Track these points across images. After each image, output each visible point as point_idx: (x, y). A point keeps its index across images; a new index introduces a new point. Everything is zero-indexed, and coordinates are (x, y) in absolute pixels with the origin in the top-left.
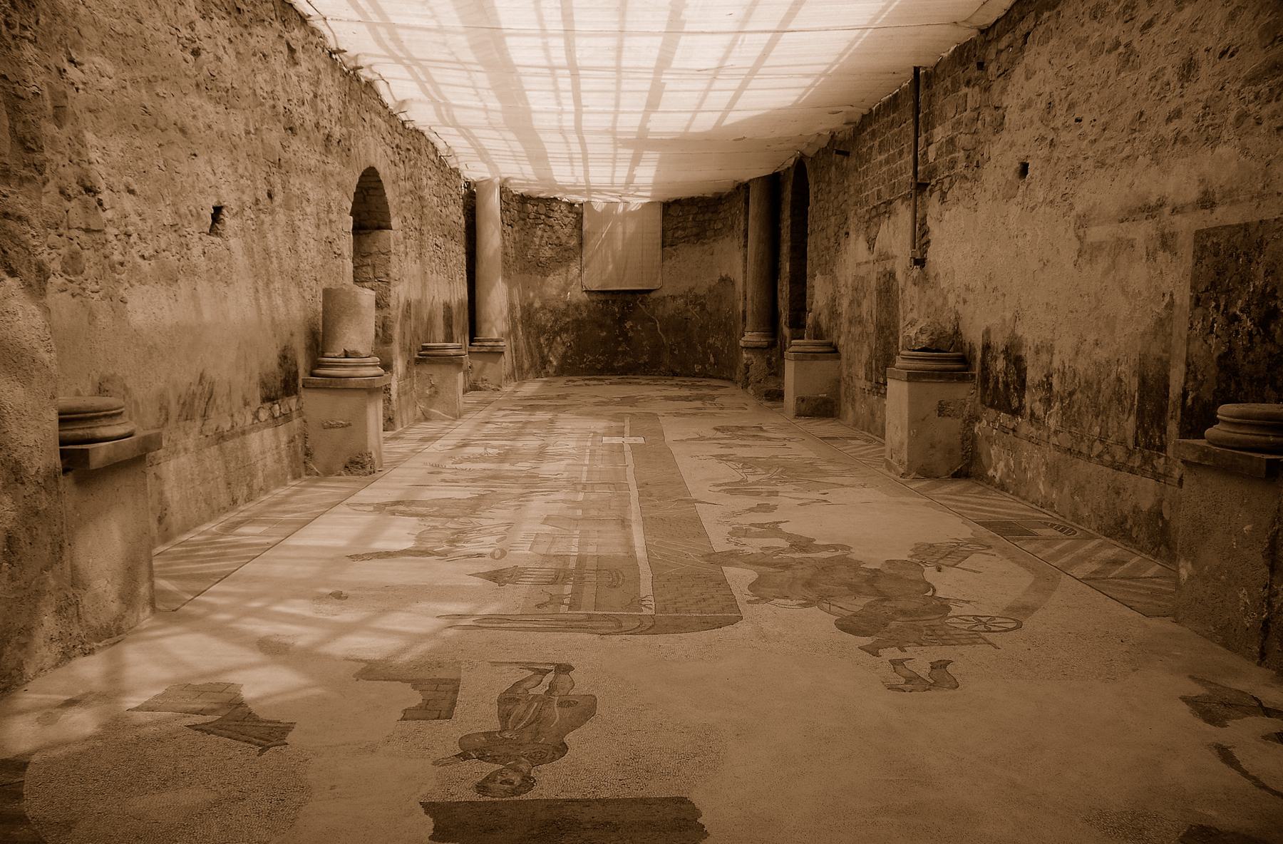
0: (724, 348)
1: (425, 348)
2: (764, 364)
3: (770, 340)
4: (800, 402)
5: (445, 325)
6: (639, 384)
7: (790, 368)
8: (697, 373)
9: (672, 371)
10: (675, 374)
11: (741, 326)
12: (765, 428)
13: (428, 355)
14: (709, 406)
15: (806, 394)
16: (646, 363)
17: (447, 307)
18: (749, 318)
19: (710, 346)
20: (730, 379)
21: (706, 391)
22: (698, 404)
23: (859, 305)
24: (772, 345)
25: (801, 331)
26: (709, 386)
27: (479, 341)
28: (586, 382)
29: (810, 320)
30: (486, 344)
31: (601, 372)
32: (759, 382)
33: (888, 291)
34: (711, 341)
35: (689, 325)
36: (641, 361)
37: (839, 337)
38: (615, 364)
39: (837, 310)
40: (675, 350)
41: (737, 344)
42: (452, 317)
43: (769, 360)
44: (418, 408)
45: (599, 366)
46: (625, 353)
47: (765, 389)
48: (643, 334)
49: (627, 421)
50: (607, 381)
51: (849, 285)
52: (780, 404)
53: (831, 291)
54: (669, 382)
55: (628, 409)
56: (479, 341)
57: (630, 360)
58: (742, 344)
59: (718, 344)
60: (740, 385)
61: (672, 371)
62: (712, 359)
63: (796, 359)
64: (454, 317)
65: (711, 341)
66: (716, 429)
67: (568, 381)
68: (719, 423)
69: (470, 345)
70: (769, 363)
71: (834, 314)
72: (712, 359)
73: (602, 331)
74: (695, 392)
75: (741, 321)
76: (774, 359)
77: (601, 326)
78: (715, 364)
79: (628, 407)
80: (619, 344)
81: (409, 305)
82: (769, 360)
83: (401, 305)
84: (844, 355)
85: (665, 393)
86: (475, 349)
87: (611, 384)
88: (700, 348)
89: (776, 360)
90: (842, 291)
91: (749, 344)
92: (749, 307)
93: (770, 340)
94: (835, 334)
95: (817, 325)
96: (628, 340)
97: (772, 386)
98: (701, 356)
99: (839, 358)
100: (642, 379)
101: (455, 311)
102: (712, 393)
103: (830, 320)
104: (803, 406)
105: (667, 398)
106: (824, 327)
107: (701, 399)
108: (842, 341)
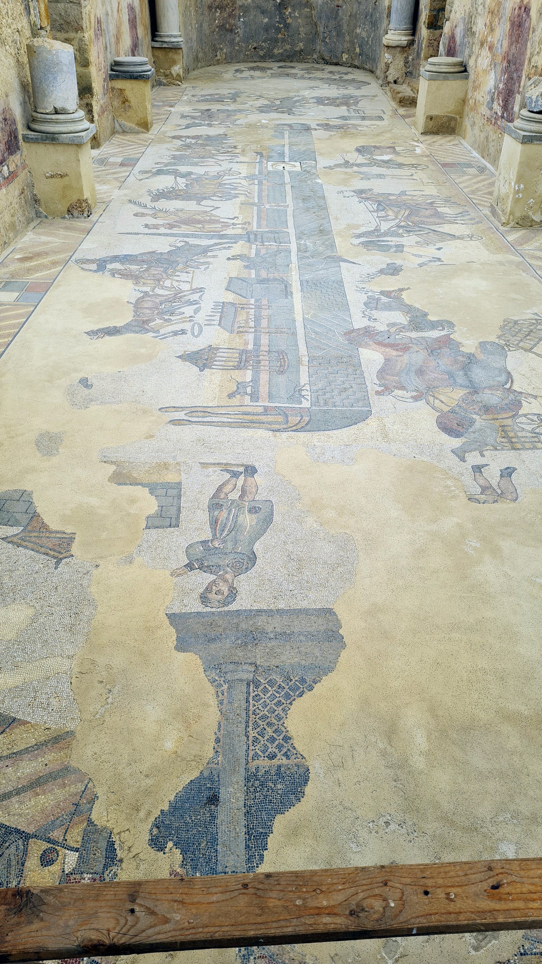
0: (368, 38)
1: (117, 64)
2: (402, 63)
3: (411, 38)
4: (429, 120)
5: (130, 28)
6: (294, 76)
7: (423, 85)
8: (344, 63)
9: (323, 59)
10: (327, 63)
11: (385, 22)
12: (397, 149)
13: (120, 71)
14: (353, 114)
15: (434, 113)
16: (302, 51)
17: (131, 8)
18: (393, 16)
19: (357, 36)
20: (372, 72)
21: (351, 91)
22: (343, 110)
23: (492, 30)
24: (411, 43)
25: (438, 32)
26: (353, 80)
27: (160, 36)
28: (252, 73)
29: (447, 28)
30: (167, 40)
31: (263, 59)
32: (395, 82)
33: (520, 26)
34: (358, 31)
35: (340, 13)
36: (298, 49)
37: (470, 56)
38: (276, 51)
39: (471, 28)
40: (326, 38)
41: (380, 40)
42: (135, 18)
43: (406, 58)
44: (115, 121)
45: (262, 53)
46: (284, 40)
47: (400, 95)
48: (299, 21)
49: (286, 136)
50: (269, 72)
51: (486, 6)
52: (411, 111)
53: (469, 6)
54: (319, 74)
55: (287, 119)
56: (160, 36)
57: (288, 47)
58: (385, 42)
59: (364, 34)
60: (380, 82)
61: (323, 59)
62: (358, 50)
63: (431, 79)
64: (137, 17)
65: (358, 31)
66: (358, 150)
67: (237, 71)
68: (361, 142)
69: (153, 40)
70: (406, 62)
71: (469, 31)
72: (358, 50)
73: (265, 17)
74: (343, 92)
75: (385, 16)
76: (410, 57)
77: (263, 12)
78: (360, 55)
79: (286, 116)
80: (278, 30)
81: (99, 22)
82: (406, 58)
83: (93, 24)
84: (472, 77)
85: (318, 93)
86: (157, 45)
87: (273, 76)
88: (347, 38)
89: (413, 59)
90: (479, 10)
91: (392, 43)
92: (396, 5)
93: (411, 38)
94: (467, 52)
95: (452, 38)
96: (287, 26)
97: (405, 90)
98: (348, 45)
99: (467, 78)
100: (298, 69)
101: (138, 10)
102: (357, 93)
103: (464, 35)
104: (431, 123)
105: (320, 101)
106: (458, 39)
107: (347, 104)
108: (471, 63)
